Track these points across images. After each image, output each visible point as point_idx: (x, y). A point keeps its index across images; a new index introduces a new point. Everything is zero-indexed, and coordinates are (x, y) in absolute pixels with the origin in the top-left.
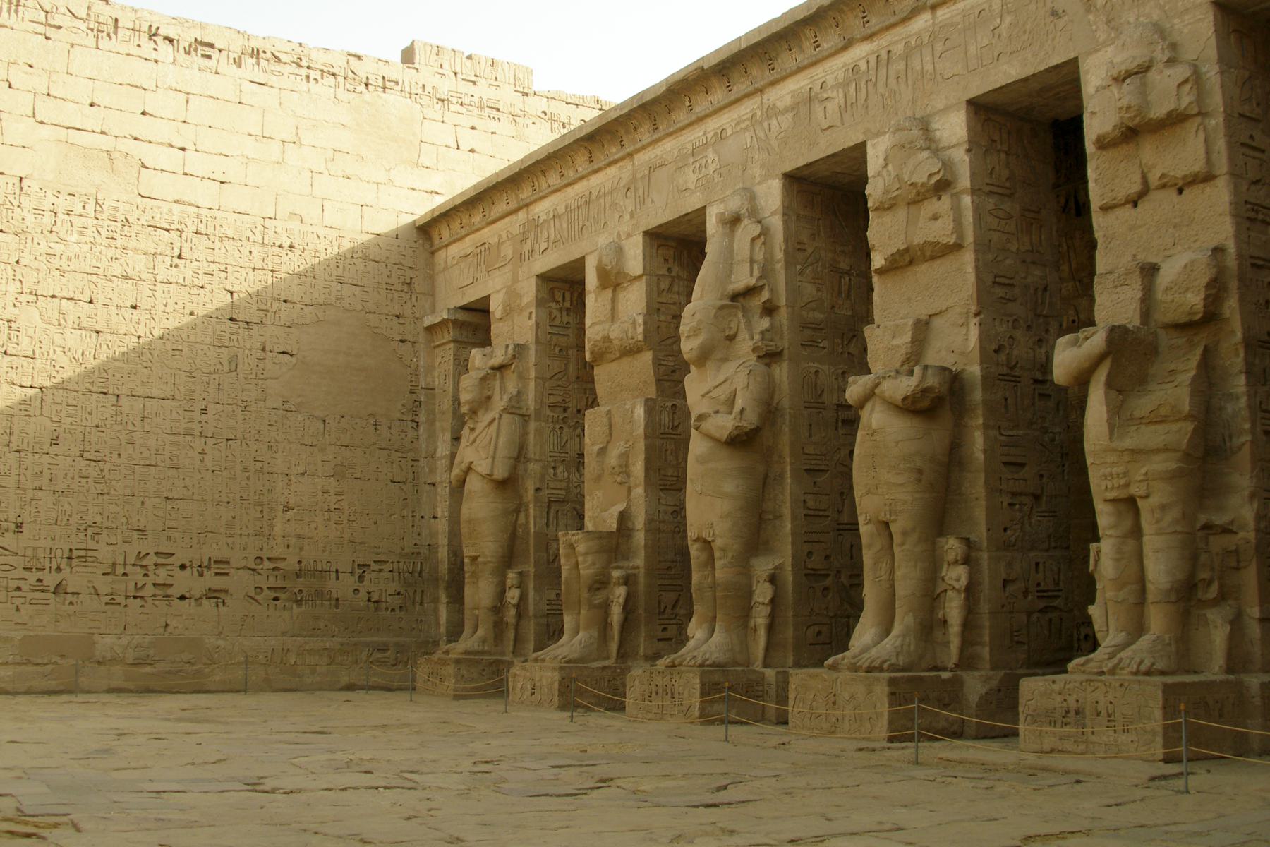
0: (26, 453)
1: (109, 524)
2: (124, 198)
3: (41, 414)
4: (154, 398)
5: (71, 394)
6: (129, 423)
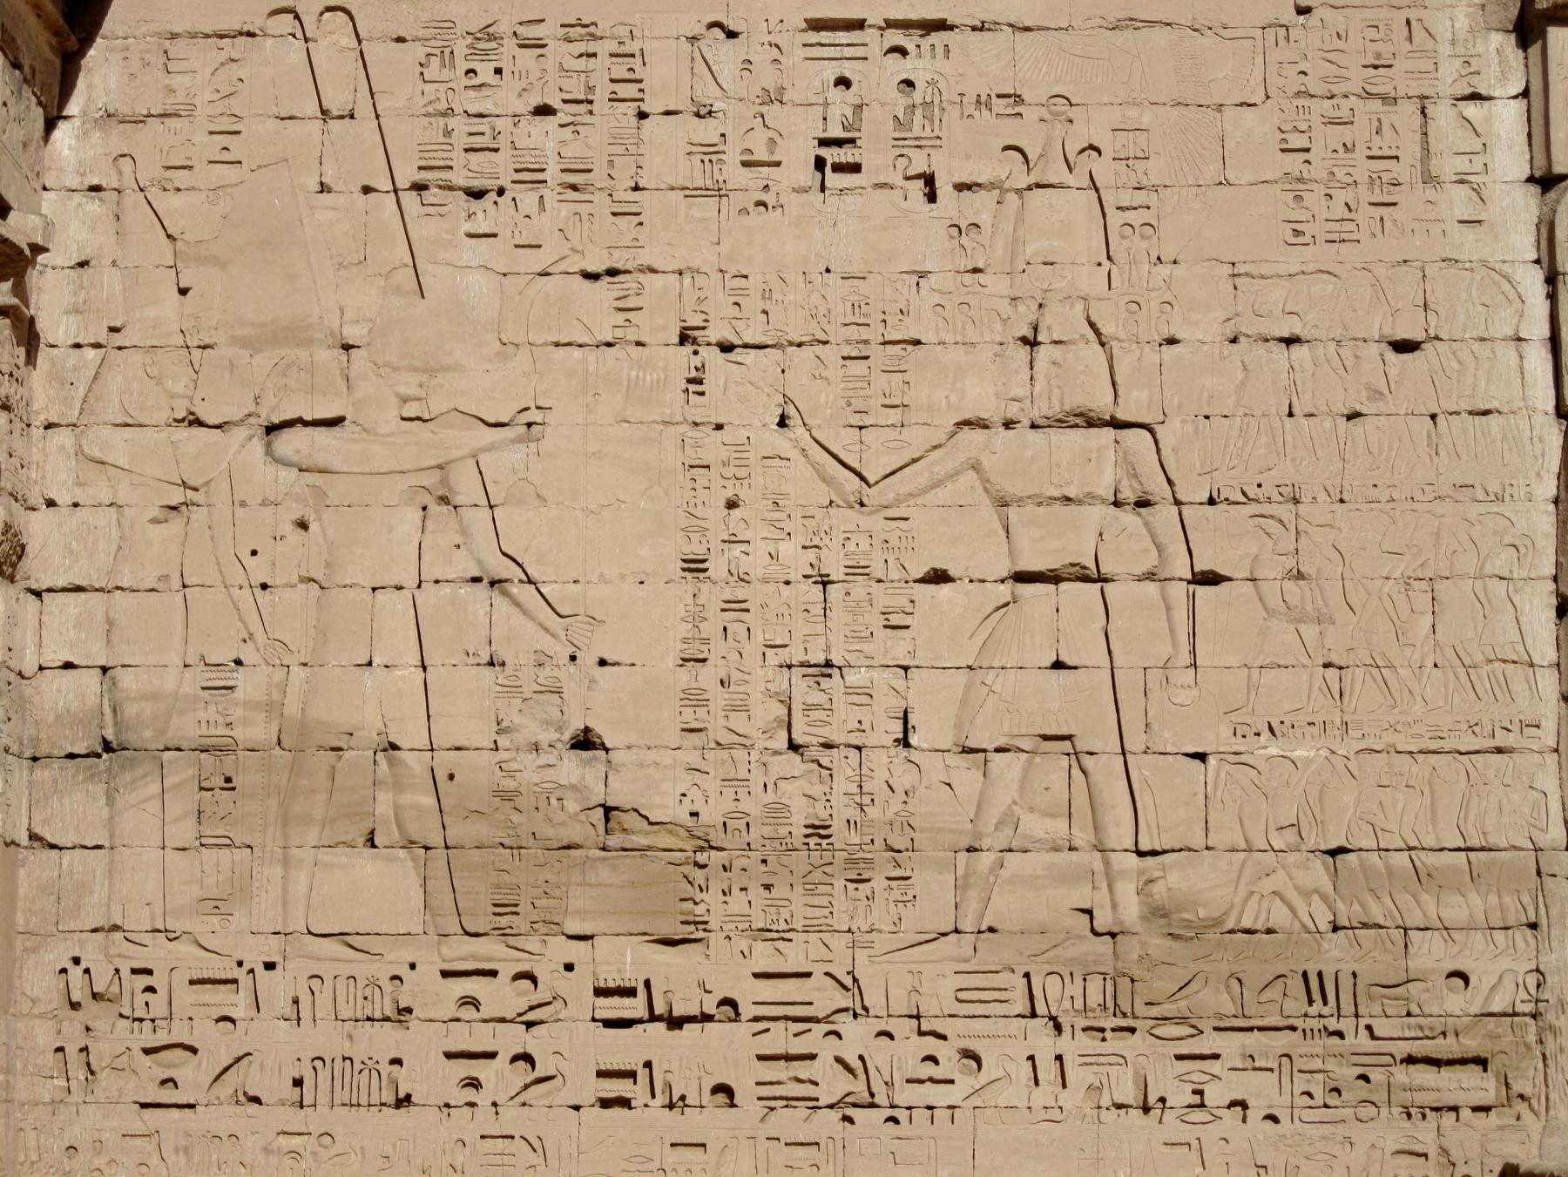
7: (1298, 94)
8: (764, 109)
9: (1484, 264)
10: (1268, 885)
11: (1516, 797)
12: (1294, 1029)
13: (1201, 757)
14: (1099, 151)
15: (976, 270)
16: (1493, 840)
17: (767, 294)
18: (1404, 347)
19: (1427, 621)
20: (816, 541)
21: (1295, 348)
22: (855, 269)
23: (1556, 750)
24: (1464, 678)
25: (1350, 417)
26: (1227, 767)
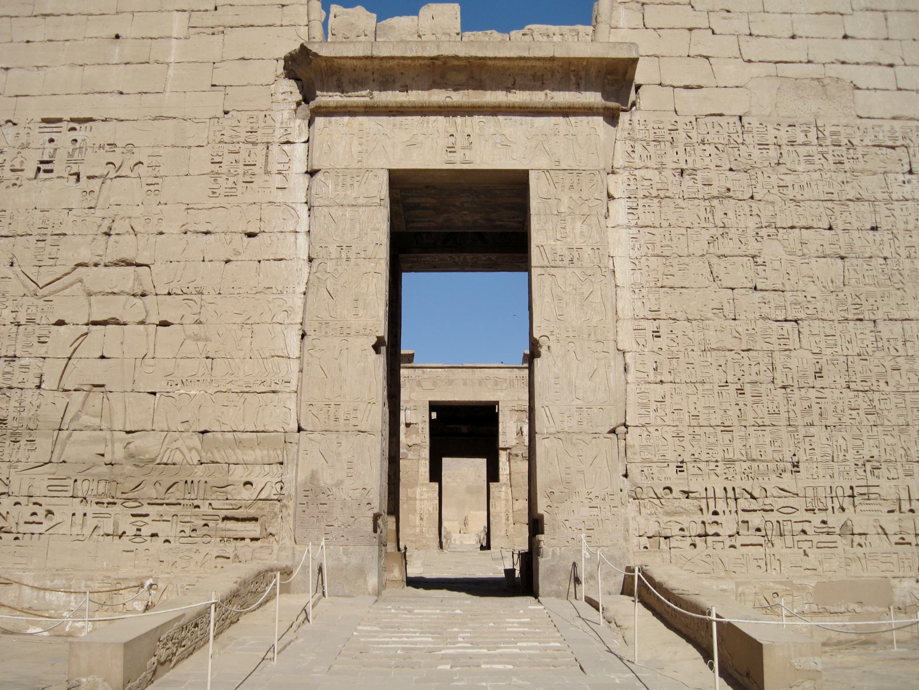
0: (792, 388)
1: (888, 457)
2: (844, 122)
3: (801, 347)
4: (912, 320)
5: (826, 324)
6: (891, 348)
7: (220, 142)
8: (21, 151)
9: (285, 203)
10: (175, 445)
11: (278, 411)
12: (180, 504)
13: (154, 394)
14: (142, 163)
15: (91, 208)
16: (267, 428)
17: (12, 218)
18: (251, 235)
19: (249, 341)
20: (16, 309)
21: (209, 235)
22: (46, 208)
23: (296, 392)
24: (261, 363)
25: (226, 262)
26: (163, 397)
